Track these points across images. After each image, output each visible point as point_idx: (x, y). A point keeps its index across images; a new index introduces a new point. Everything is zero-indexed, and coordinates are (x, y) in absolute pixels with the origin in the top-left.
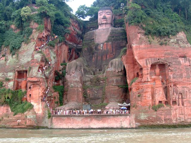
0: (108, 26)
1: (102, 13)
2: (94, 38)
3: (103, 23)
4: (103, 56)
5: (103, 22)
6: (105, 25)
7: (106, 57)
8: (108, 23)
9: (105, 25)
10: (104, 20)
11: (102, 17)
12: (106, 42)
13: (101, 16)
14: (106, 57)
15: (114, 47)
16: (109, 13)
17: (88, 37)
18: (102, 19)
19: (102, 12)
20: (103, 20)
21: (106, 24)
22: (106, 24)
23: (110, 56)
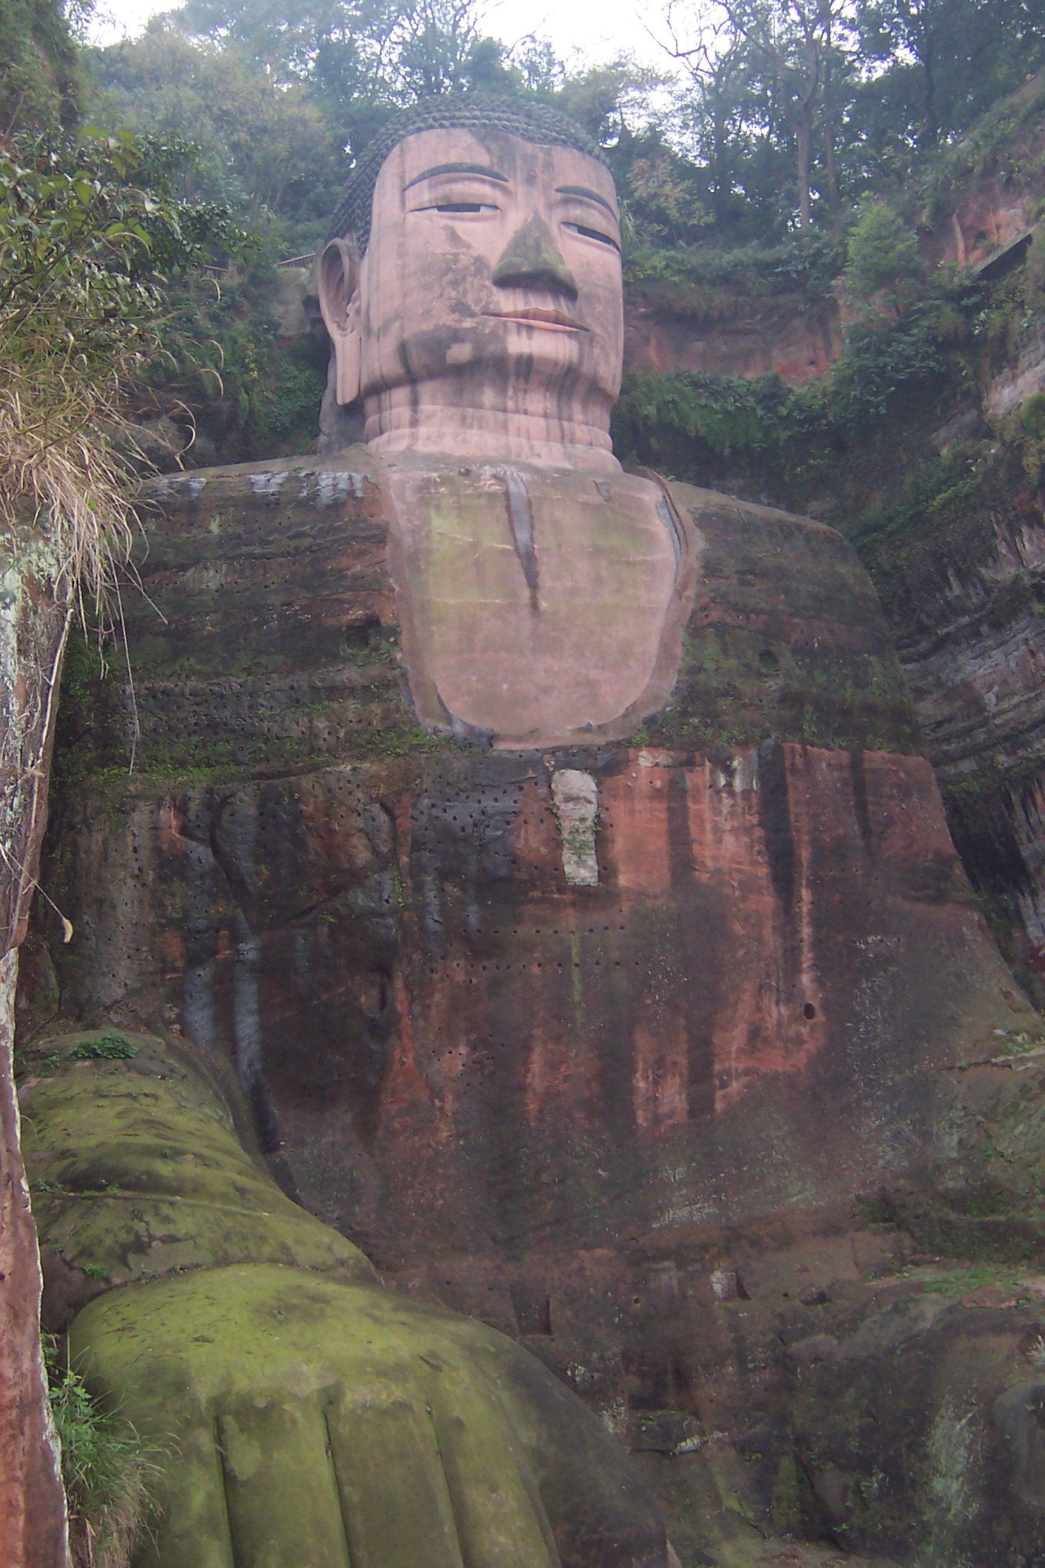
0: (591, 443)
1: (494, 177)
2: (387, 620)
3: (526, 368)
4: (643, 1041)
5: (518, 345)
6: (551, 405)
7: (701, 1076)
8: (595, 390)
9: (538, 402)
10: (548, 305)
11: (489, 239)
12: (657, 730)
13: (466, 226)
14: (701, 1076)
15: (805, 854)
16: (597, 219)
17: (212, 579)
18: (507, 281)
19: (483, 159)
20: (509, 302)
21: (565, 383)
22: (565, 383)
23: (756, 1036)
